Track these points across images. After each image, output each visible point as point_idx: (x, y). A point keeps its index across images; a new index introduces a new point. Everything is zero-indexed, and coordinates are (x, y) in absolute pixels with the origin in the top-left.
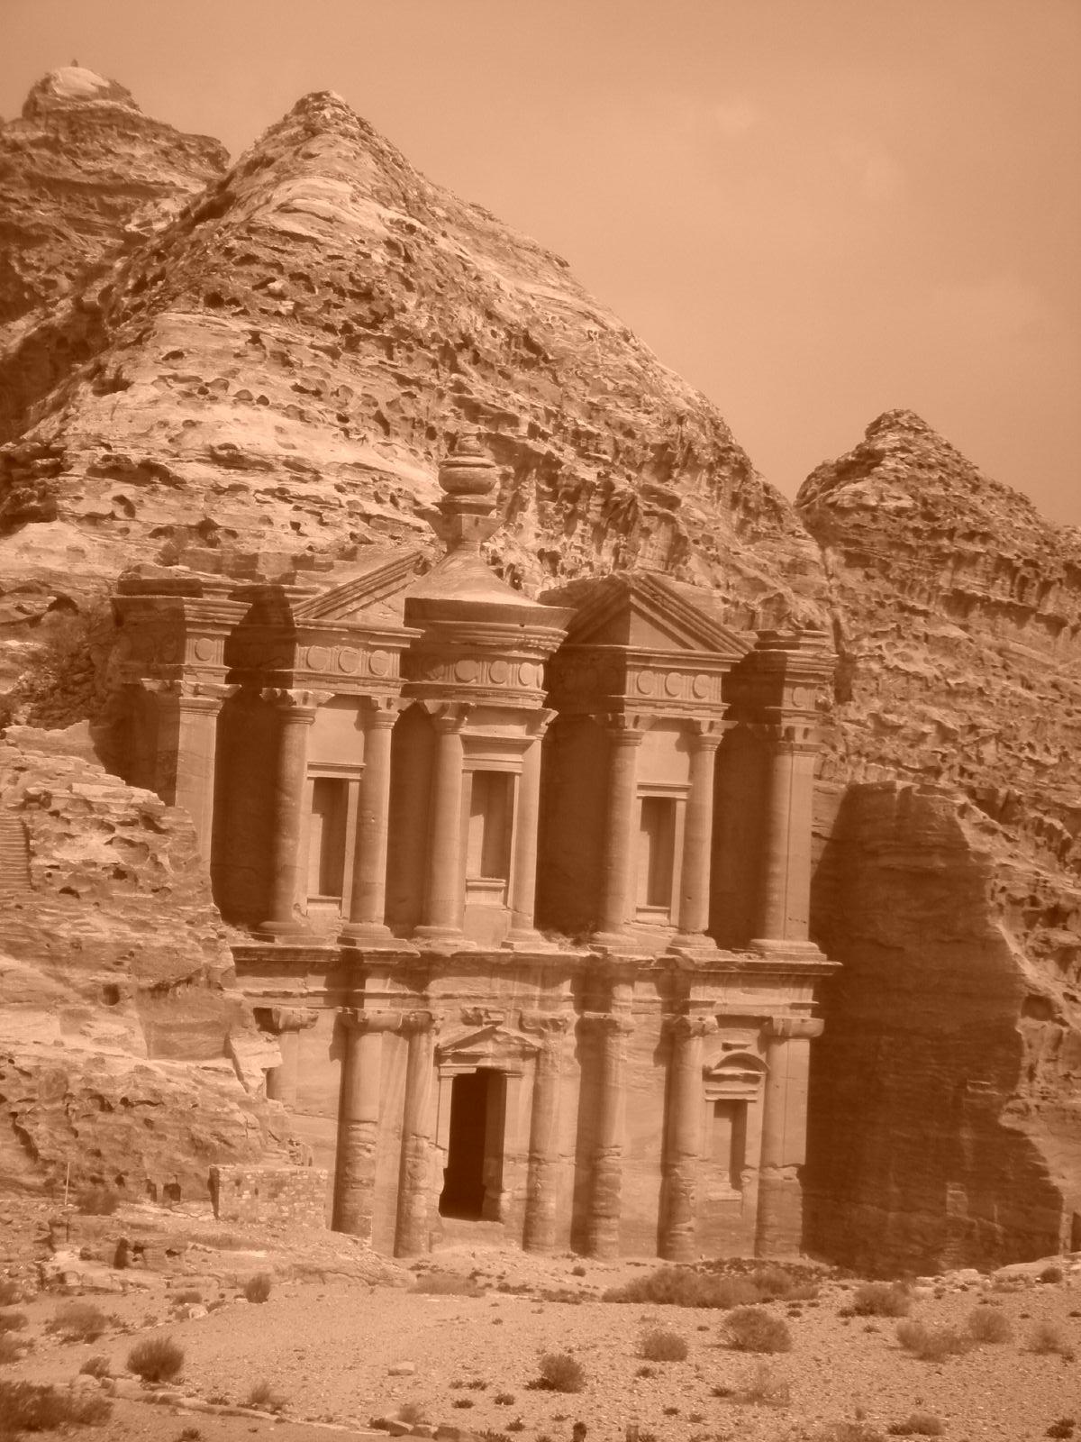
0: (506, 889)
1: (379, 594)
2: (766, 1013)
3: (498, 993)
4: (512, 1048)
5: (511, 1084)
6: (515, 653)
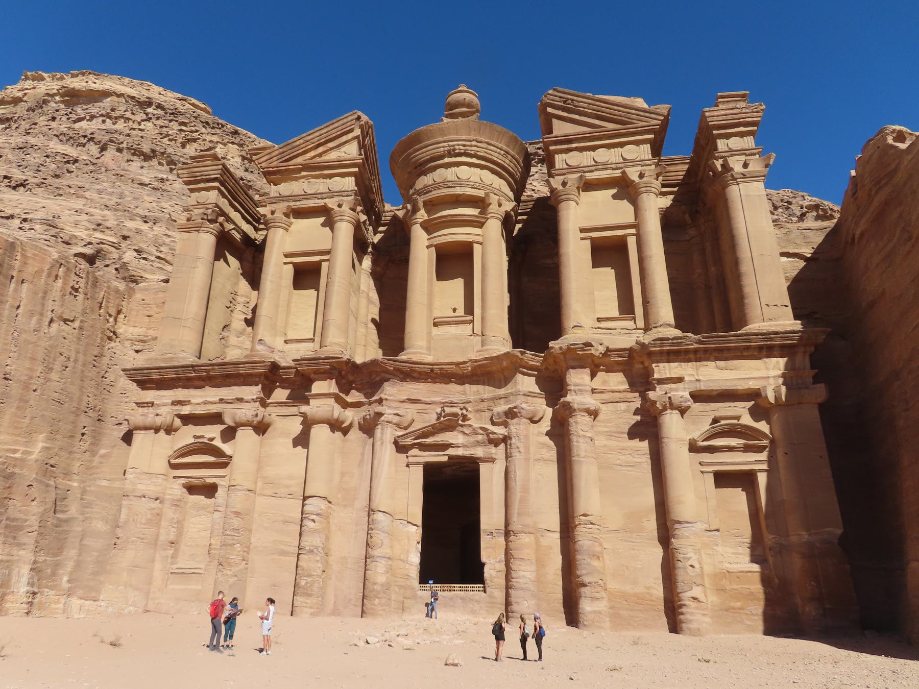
0: (473, 321)
1: (331, 145)
2: (753, 385)
3: (471, 398)
4: (480, 437)
5: (484, 468)
6: (447, 160)
